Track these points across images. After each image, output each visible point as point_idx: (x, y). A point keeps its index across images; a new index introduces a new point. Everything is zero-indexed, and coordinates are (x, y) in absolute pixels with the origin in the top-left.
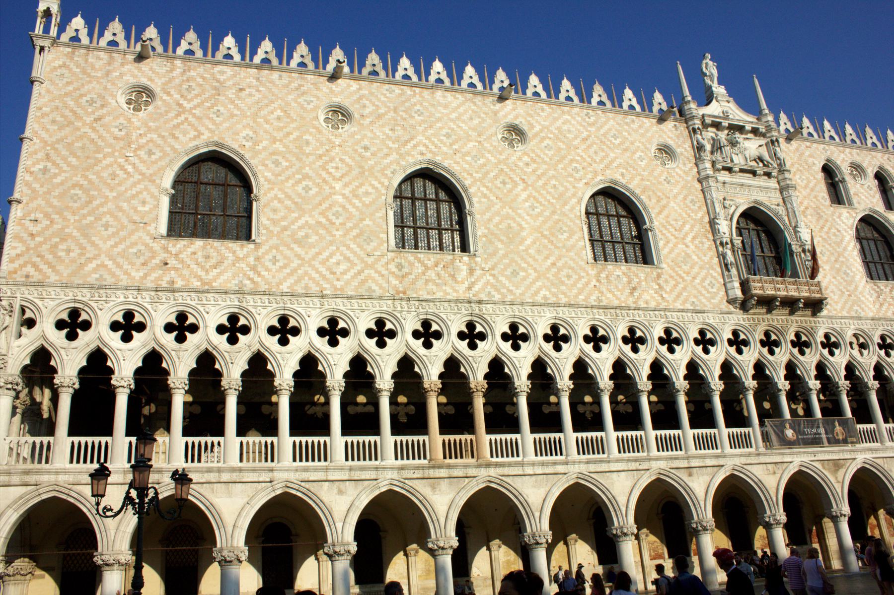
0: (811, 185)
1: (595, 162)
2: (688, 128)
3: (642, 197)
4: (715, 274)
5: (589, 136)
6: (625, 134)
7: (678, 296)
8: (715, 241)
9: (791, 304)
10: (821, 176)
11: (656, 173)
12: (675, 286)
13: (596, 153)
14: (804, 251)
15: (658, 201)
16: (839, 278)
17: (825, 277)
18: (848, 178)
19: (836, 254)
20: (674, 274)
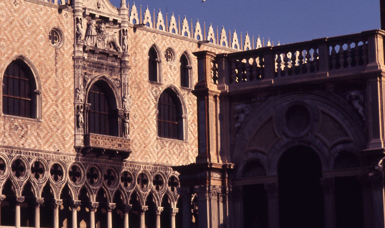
0: (140, 64)
1: (15, 41)
2: (74, 16)
3: (38, 69)
4: (70, 128)
5: (14, 20)
6: (35, 19)
7: (47, 142)
8: (74, 104)
9: (110, 153)
10: (147, 58)
11: (48, 52)
12: (47, 134)
13: (16, 34)
14: (125, 114)
15: (46, 73)
16: (141, 134)
17: (133, 134)
18: (163, 60)
19: (143, 117)
20: (47, 126)
